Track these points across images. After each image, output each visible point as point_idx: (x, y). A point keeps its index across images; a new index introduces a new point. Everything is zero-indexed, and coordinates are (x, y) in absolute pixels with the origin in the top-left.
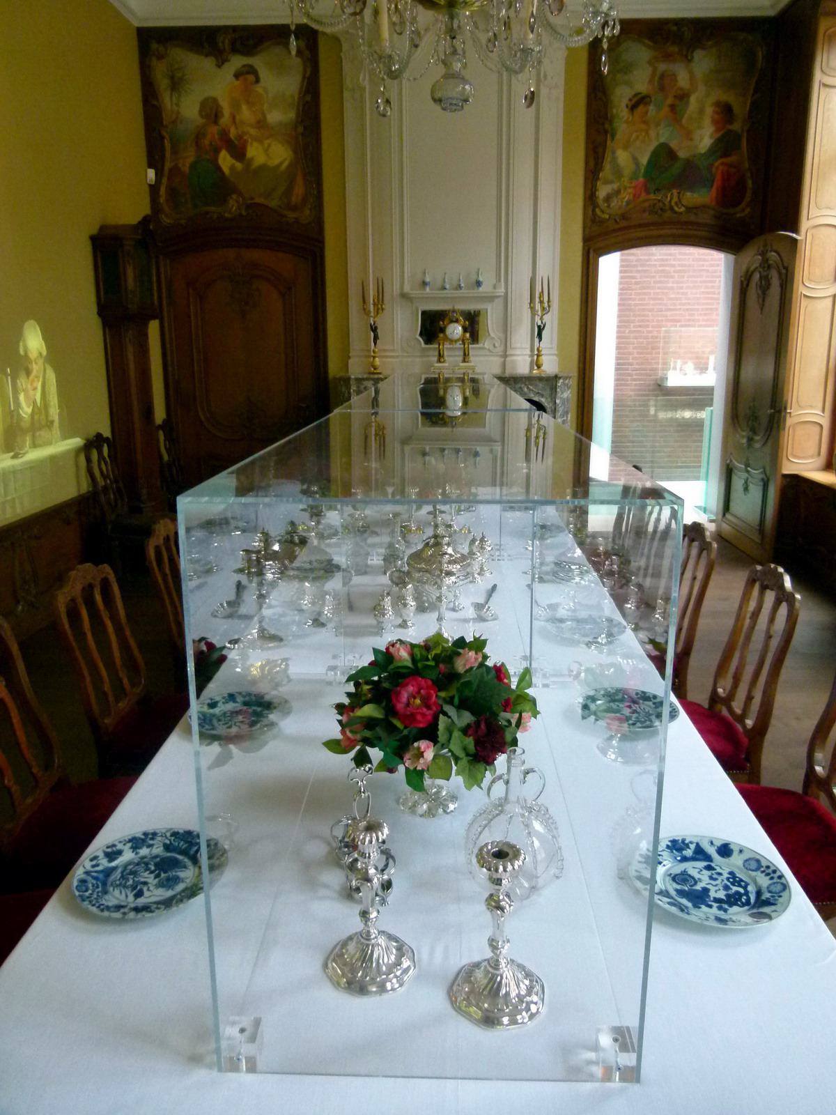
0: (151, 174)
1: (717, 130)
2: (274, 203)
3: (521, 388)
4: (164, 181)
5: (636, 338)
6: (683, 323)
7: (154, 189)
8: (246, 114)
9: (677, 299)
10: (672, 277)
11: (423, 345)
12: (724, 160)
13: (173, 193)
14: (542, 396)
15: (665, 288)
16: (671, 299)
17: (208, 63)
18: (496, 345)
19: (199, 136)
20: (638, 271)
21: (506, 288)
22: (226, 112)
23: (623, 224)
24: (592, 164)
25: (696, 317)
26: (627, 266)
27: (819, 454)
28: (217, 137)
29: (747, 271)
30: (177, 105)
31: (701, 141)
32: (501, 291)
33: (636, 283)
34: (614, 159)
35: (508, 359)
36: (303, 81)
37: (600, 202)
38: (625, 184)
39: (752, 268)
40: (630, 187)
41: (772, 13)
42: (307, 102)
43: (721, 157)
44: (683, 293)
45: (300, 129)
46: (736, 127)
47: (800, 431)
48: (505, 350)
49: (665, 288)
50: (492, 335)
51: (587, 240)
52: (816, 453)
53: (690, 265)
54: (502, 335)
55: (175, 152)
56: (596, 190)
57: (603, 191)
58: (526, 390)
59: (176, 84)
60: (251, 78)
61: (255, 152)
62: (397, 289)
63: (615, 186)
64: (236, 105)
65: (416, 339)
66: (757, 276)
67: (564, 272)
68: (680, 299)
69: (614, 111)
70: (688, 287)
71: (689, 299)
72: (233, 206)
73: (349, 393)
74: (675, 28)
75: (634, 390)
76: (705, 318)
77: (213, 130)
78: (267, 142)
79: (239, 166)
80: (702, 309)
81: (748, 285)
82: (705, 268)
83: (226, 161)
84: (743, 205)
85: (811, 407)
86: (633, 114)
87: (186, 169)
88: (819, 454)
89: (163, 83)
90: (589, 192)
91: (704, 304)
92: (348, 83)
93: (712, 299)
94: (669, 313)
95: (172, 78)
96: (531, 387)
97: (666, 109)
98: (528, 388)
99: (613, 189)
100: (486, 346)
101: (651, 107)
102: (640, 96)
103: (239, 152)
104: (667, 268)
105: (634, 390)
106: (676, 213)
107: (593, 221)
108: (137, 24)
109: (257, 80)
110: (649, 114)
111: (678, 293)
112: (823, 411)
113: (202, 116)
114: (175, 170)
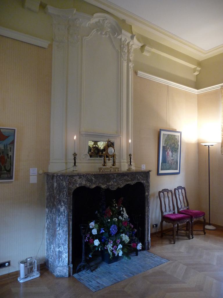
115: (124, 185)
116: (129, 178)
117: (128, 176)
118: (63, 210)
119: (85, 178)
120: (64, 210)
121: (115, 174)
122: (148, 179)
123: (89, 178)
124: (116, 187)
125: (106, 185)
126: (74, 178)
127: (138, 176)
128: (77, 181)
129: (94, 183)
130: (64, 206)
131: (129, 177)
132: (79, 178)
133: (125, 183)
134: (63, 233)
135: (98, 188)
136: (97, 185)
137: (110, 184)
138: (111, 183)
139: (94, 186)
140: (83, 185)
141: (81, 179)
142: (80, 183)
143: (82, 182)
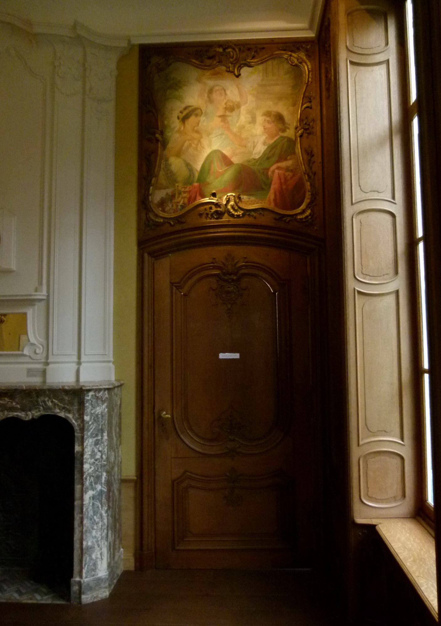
1: (271, 136)
3: (44, 402)
12: (279, 164)
14: (69, 412)
18: (38, 351)
23: (178, 227)
27: (404, 496)
31: (254, 147)
34: (168, 166)
35: (51, 366)
38: (180, 188)
40: (185, 192)
43: (278, 162)
47: (375, 464)
48: (47, 357)
50: (32, 340)
52: (400, 493)
54: (42, 340)
56: (149, 195)
57: (157, 196)
58: (50, 404)
63: (169, 191)
84: (303, 207)
85: (385, 432)
88: (404, 496)
96: (56, 401)
98: (52, 402)
99: (167, 194)
100: (26, 352)
106: (232, 216)
112: (402, 439)
127: (46, 399)
131: (17, 400)
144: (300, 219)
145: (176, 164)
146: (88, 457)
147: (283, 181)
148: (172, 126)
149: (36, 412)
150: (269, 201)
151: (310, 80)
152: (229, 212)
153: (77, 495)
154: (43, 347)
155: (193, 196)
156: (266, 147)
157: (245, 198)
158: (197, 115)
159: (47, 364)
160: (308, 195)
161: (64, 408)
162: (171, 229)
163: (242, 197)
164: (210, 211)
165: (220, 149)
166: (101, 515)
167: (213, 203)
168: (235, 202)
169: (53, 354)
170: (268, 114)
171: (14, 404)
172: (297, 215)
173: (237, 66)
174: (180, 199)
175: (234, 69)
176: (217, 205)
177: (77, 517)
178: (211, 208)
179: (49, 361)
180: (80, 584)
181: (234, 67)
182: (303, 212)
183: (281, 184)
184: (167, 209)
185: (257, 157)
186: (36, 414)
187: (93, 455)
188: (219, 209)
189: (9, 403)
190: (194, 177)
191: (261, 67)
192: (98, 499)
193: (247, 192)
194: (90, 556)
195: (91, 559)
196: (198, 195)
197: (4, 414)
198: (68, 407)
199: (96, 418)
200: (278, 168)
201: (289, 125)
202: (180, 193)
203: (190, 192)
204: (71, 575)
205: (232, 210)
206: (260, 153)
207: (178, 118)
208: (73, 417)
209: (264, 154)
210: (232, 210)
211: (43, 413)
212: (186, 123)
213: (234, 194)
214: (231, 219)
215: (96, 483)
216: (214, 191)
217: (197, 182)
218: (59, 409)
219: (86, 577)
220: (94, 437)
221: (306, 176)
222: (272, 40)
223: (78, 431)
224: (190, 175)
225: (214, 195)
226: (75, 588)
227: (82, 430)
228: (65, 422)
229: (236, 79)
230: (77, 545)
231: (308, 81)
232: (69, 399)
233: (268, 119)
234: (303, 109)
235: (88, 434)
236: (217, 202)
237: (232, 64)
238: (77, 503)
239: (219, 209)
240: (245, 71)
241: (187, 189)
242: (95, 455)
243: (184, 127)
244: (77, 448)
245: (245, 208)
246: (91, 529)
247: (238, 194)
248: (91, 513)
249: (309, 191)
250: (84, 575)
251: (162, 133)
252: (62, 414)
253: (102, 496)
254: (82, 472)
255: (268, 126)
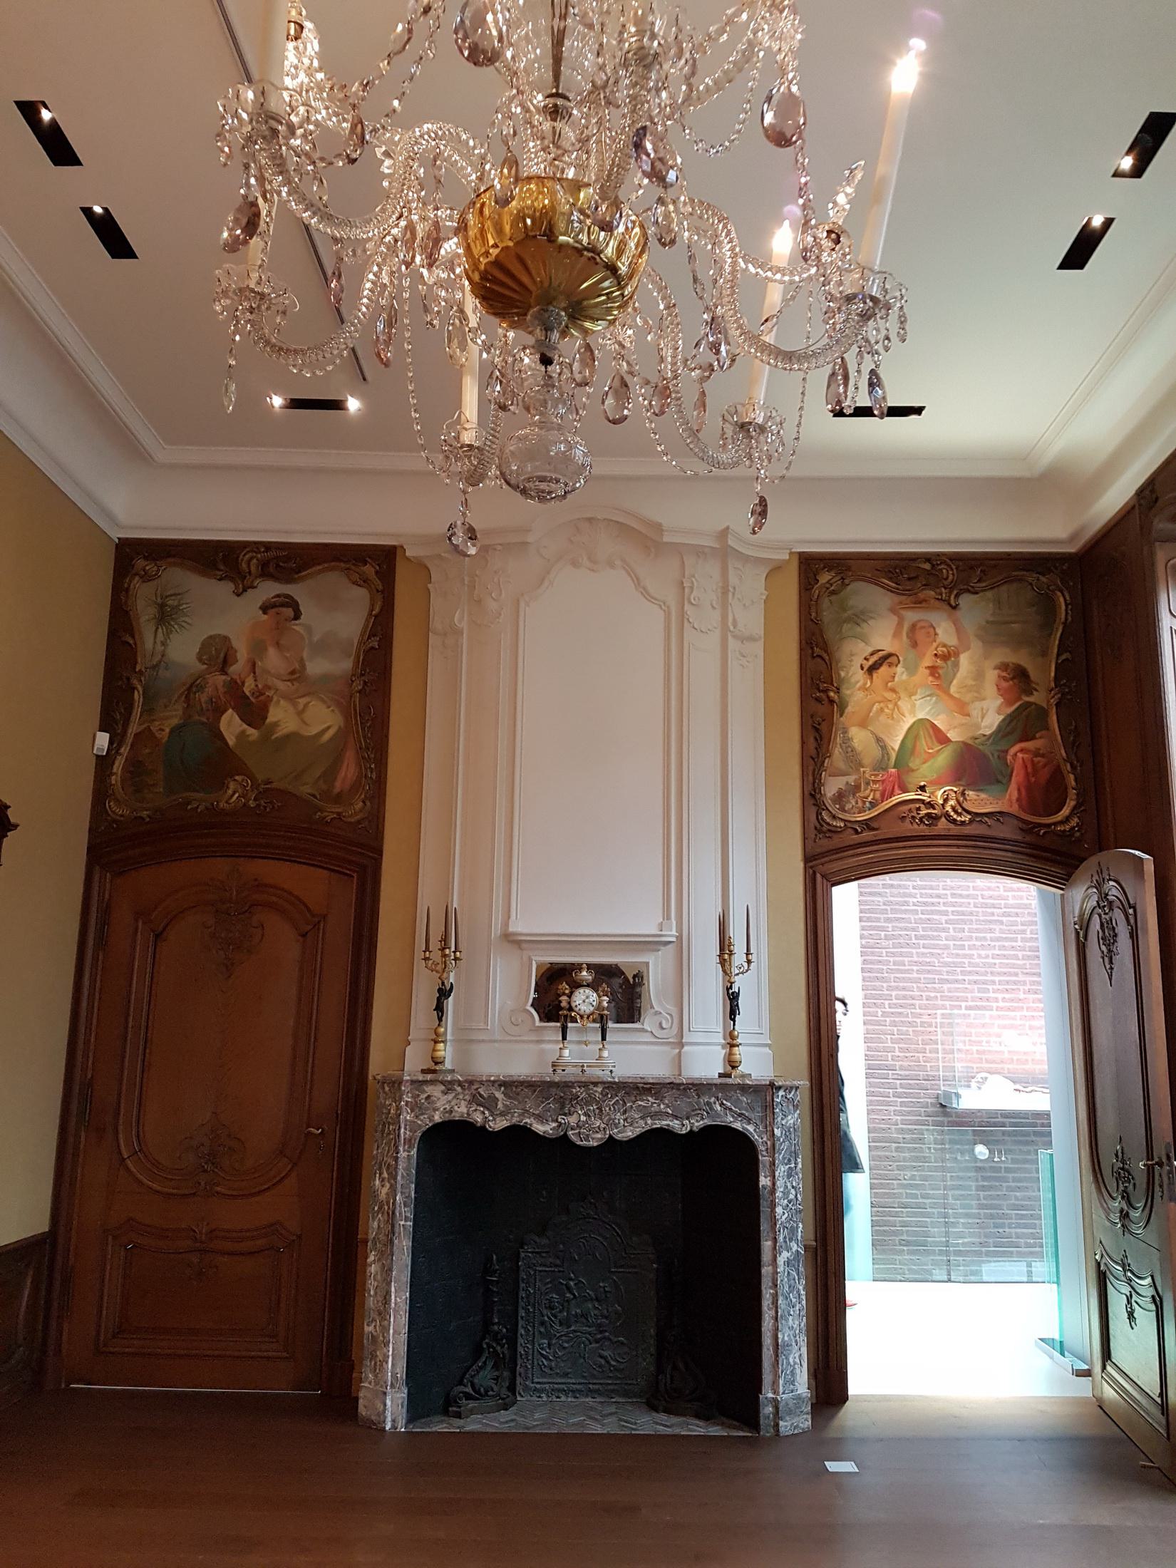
0: (103, 740)
1: (1009, 702)
2: (305, 790)
3: (708, 1104)
4: (125, 750)
5: (894, 1024)
6: (971, 1004)
7: (104, 763)
8: (273, 660)
9: (956, 965)
10: (944, 930)
11: (538, 1023)
12: (1023, 745)
13: (135, 768)
14: (749, 1121)
15: (935, 946)
16: (947, 964)
17: (222, 590)
18: (664, 1026)
19: (193, 687)
20: (888, 920)
21: (680, 929)
22: (242, 654)
23: (867, 835)
24: (812, 744)
25: (992, 995)
26: (870, 911)
28: (221, 690)
29: (1081, 915)
30: (163, 644)
32: (671, 933)
33: (886, 938)
34: (847, 740)
35: (686, 1048)
36: (367, 620)
37: (829, 803)
38: (867, 776)
39: (1088, 912)
41: (1072, 549)
42: (373, 648)
43: (1021, 741)
44: (965, 956)
45: (358, 686)
46: (1037, 698)
48: (681, 1034)
49: (935, 946)
51: (810, 859)
53: (971, 914)
54: (674, 1010)
55: (148, 710)
56: (821, 784)
57: (831, 787)
59: (166, 616)
60: (289, 612)
61: (282, 716)
62: (496, 931)
63: (851, 779)
64: (258, 649)
65: (528, 1010)
66: (1096, 925)
67: (773, 906)
68: (961, 965)
69: (843, 674)
70: (971, 948)
71: (977, 965)
72: (233, 794)
73: (398, 1108)
74: (927, 566)
75: (900, 1113)
76: (1007, 996)
77: (218, 680)
78: (302, 701)
79: (253, 733)
80: (1000, 983)
81: (1086, 937)
82: (996, 918)
83: (231, 725)
84: (1065, 811)
86: (871, 679)
87: (164, 736)
89: (144, 613)
90: (809, 788)
91: (999, 974)
92: (437, 623)
93: (1013, 966)
94: (945, 986)
95: (162, 606)
97: (923, 672)
98: (722, 1104)
101: (899, 669)
102: (881, 654)
103: (254, 712)
104: (935, 917)
105: (900, 1113)
106: (954, 821)
107: (819, 830)
108: (116, 534)
109: (297, 616)
110: (896, 679)
111: (958, 955)
113: (200, 660)
114: (145, 736)
115: (638, 1131)
116: (662, 1106)
117: (659, 1096)
118: (384, 1196)
119: (467, 1092)
120: (387, 1194)
121: (595, 1084)
122: (956, 1113)
123: (481, 1095)
124: (599, 1136)
125: (554, 1125)
126: (424, 1091)
127: (713, 1100)
128: (434, 1102)
129: (502, 1114)
130: (389, 1182)
132: (445, 1093)
133: (646, 1124)
134: (382, 1275)
135: (519, 1133)
136: (515, 1120)
137: (572, 1120)
138: (575, 1115)
139: (498, 1124)
140: (457, 1115)
141: (450, 1097)
142: (448, 1107)
143: (456, 1108)
144: (1060, 830)
145: (859, 737)
146: (781, 1195)
147: (1030, 770)
148: (853, 680)
149: (697, 1121)
150: (1010, 800)
151: (1070, 619)
152: (947, 815)
153: (766, 1256)
154: (672, 1020)
155: (889, 788)
156: (1001, 717)
157: (971, 794)
158: (890, 665)
159: (681, 1045)
160: (1072, 793)
161: (740, 1115)
162: (856, 838)
163: (967, 792)
164: (919, 814)
165: (927, 717)
166: (798, 1291)
167: (922, 801)
168: (958, 800)
169: (690, 1031)
170: (1004, 667)
171: (662, 1106)
172: (1055, 824)
173: (955, 592)
174: (868, 792)
175: (950, 597)
176: (930, 805)
177: (767, 1294)
178: (919, 809)
179: (684, 1041)
180: (776, 1404)
181: (950, 593)
182: (1067, 819)
183: (1027, 774)
184: (848, 807)
185: (988, 732)
186: (696, 1124)
187: (786, 1194)
188: (931, 811)
189: (655, 1105)
190: (889, 760)
191: (989, 594)
192: (794, 1266)
193: (974, 784)
194: (787, 1358)
195: (788, 1363)
196: (896, 787)
197: (646, 1124)
198: (747, 1114)
199: (787, 1131)
200: (1022, 750)
201: (1038, 684)
202: (868, 784)
203: (883, 781)
204: (759, 1390)
205: (952, 814)
206: (992, 725)
207: (862, 668)
208: (755, 1130)
209: (999, 728)
210: (952, 814)
211: (708, 1122)
212: (875, 675)
213: (955, 789)
214: (952, 826)
215: (791, 1240)
216: (922, 784)
217: (894, 767)
218: (733, 1117)
219: (783, 1393)
220: (786, 1165)
221: (1068, 765)
222: (1009, 554)
223: (764, 1153)
224: (883, 756)
225: (922, 788)
226: (768, 1410)
227: (773, 1150)
228: (743, 1137)
229: (953, 611)
230: (767, 1341)
231: (1066, 619)
232: (749, 1101)
233: (1004, 674)
234: (1060, 661)
235: (779, 1157)
236: (929, 800)
237: (945, 588)
238: (766, 1270)
239: (931, 811)
240: (966, 600)
241: (879, 778)
242: (789, 1192)
243: (872, 682)
244: (764, 1181)
245: (974, 810)
246: (786, 1314)
247: (962, 788)
248: (786, 1288)
249: (1073, 789)
250: (781, 1390)
251: (838, 690)
252: (737, 1125)
253: (799, 1262)
254: (774, 1221)
255: (1004, 684)
